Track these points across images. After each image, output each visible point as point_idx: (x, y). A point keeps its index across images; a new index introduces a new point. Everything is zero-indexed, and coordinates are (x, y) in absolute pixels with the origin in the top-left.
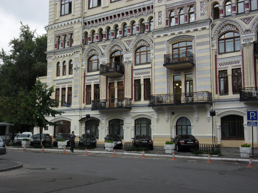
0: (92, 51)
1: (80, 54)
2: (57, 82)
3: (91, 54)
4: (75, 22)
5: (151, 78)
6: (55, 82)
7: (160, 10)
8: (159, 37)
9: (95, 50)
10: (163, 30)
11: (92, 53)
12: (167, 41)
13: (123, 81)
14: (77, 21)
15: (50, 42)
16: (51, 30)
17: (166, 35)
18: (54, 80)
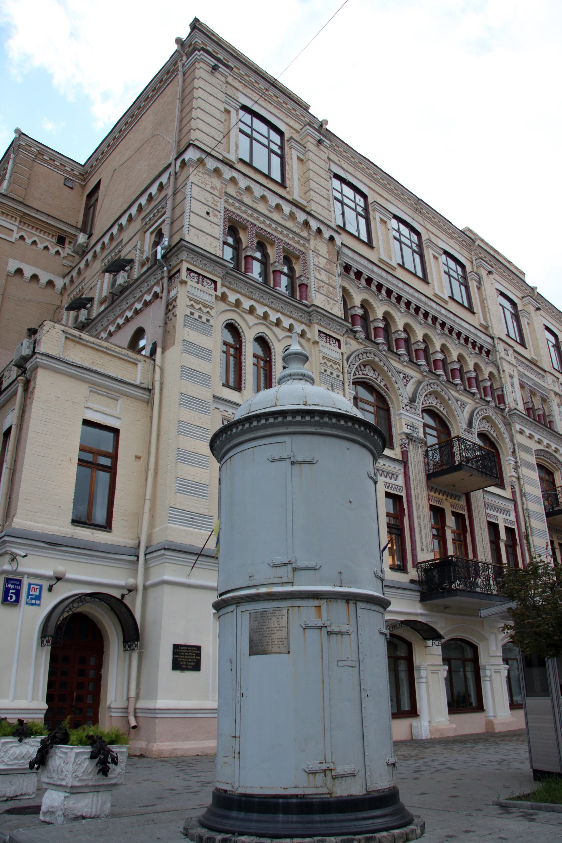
0: (365, 366)
1: (342, 350)
2: (231, 411)
3: (363, 374)
4: (319, 231)
5: (515, 527)
6: (222, 408)
7: (511, 372)
8: (521, 432)
9: (374, 371)
10: (529, 423)
11: (365, 372)
12: (535, 451)
13: (465, 513)
14: (327, 234)
15: (204, 215)
16: (207, 172)
17: (531, 437)
18: (214, 397)
